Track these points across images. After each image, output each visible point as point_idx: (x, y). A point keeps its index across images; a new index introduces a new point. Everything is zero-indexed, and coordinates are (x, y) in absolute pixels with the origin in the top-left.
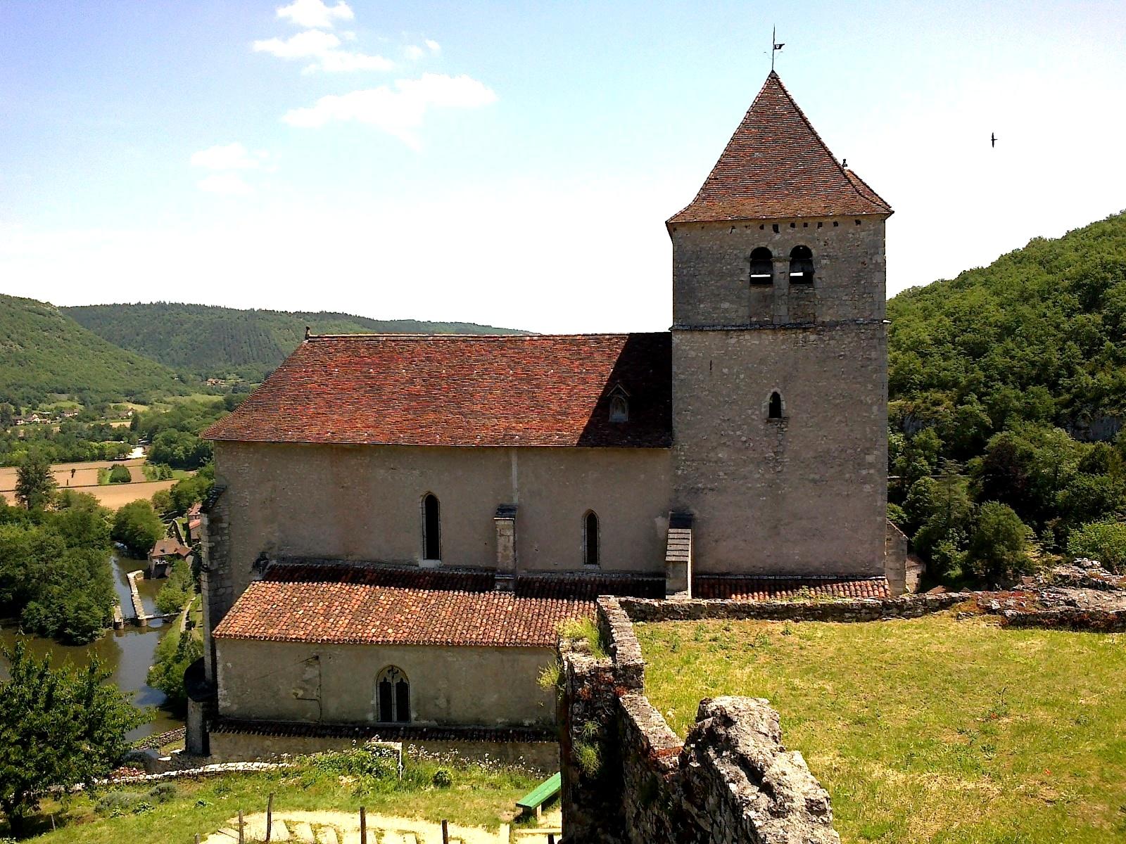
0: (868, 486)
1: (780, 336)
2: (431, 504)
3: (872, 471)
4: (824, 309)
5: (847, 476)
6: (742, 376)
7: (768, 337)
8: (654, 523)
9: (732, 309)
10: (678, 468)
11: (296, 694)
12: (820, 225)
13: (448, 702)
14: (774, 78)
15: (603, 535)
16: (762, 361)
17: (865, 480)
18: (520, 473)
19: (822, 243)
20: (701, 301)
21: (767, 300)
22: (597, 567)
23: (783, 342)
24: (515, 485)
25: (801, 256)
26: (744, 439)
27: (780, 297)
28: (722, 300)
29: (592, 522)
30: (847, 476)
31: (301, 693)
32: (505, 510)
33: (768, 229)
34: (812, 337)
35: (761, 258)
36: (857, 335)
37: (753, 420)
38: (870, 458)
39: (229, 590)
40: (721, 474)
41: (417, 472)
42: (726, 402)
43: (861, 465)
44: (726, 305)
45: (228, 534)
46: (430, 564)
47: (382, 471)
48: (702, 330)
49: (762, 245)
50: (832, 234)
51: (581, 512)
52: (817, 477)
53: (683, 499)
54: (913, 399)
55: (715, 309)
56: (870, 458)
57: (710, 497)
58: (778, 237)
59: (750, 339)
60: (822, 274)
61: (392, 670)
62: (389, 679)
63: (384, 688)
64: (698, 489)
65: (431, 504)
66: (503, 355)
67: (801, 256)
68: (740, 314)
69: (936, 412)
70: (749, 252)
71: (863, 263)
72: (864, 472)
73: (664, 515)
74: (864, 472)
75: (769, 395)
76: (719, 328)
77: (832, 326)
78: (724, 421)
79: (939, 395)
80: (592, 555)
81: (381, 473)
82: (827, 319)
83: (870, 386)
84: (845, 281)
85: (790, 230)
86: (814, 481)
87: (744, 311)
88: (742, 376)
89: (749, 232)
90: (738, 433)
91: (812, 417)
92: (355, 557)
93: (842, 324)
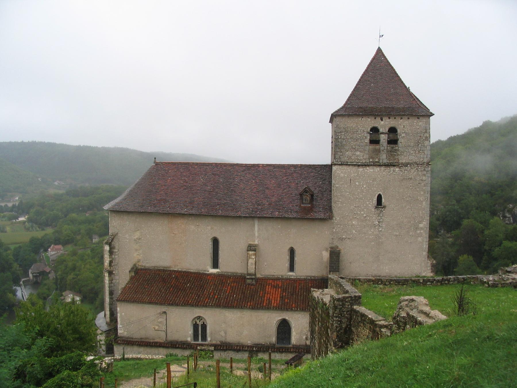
0: (420, 238)
1: (383, 168)
2: (216, 242)
3: (422, 231)
4: (403, 156)
5: (411, 233)
6: (365, 186)
7: (377, 169)
8: (321, 254)
9: (362, 156)
10: (334, 228)
11: (155, 328)
12: (401, 118)
13: (226, 333)
15: (296, 259)
16: (374, 180)
17: (420, 235)
18: (259, 229)
19: (402, 127)
21: (378, 152)
22: (294, 274)
23: (384, 171)
24: (257, 234)
25: (393, 130)
26: (365, 215)
27: (383, 151)
28: (356, 151)
29: (292, 251)
30: (411, 233)
31: (157, 328)
32: (252, 248)
34: (397, 169)
35: (375, 130)
36: (417, 169)
37: (369, 207)
38: (421, 225)
39: (117, 281)
40: (354, 231)
41: (209, 228)
42: (357, 198)
43: (417, 228)
44: (358, 153)
45: (118, 255)
46: (215, 271)
47: (193, 227)
48: (347, 165)
51: (288, 247)
52: (397, 234)
53: (336, 243)
55: (353, 154)
58: (382, 123)
59: (370, 170)
60: (402, 141)
61: (199, 318)
62: (198, 322)
63: (195, 327)
64: (343, 238)
65: (216, 242)
66: (249, 173)
67: (393, 130)
68: (365, 157)
71: (420, 136)
72: (418, 232)
73: (326, 250)
74: (418, 232)
75: (377, 195)
76: (355, 163)
77: (406, 165)
78: (356, 207)
80: (292, 268)
81: (192, 227)
82: (404, 161)
83: (422, 193)
84: (412, 144)
85: (388, 120)
86: (396, 236)
88: (365, 186)
89: (369, 120)
90: (362, 213)
91: (396, 206)
92: (178, 267)
93: (410, 164)
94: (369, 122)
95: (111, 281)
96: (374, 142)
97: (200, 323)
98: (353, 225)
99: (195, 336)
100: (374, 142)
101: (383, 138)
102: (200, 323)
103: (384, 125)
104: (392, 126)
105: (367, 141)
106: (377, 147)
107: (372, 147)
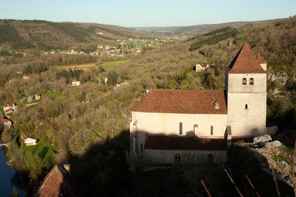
7: (245, 94)
9: (239, 89)
38: (263, 116)
43: (261, 117)
56: (263, 116)
57: (234, 123)
59: (242, 94)
61: (177, 154)
63: (176, 157)
67: (252, 79)
80: (212, 134)
87: (241, 89)
94: (243, 76)
95: (136, 140)
96: (244, 84)
97: (178, 156)
98: (236, 116)
99: (176, 162)
101: (248, 82)
102: (178, 156)
103: (248, 76)
106: (245, 86)
107: (243, 86)
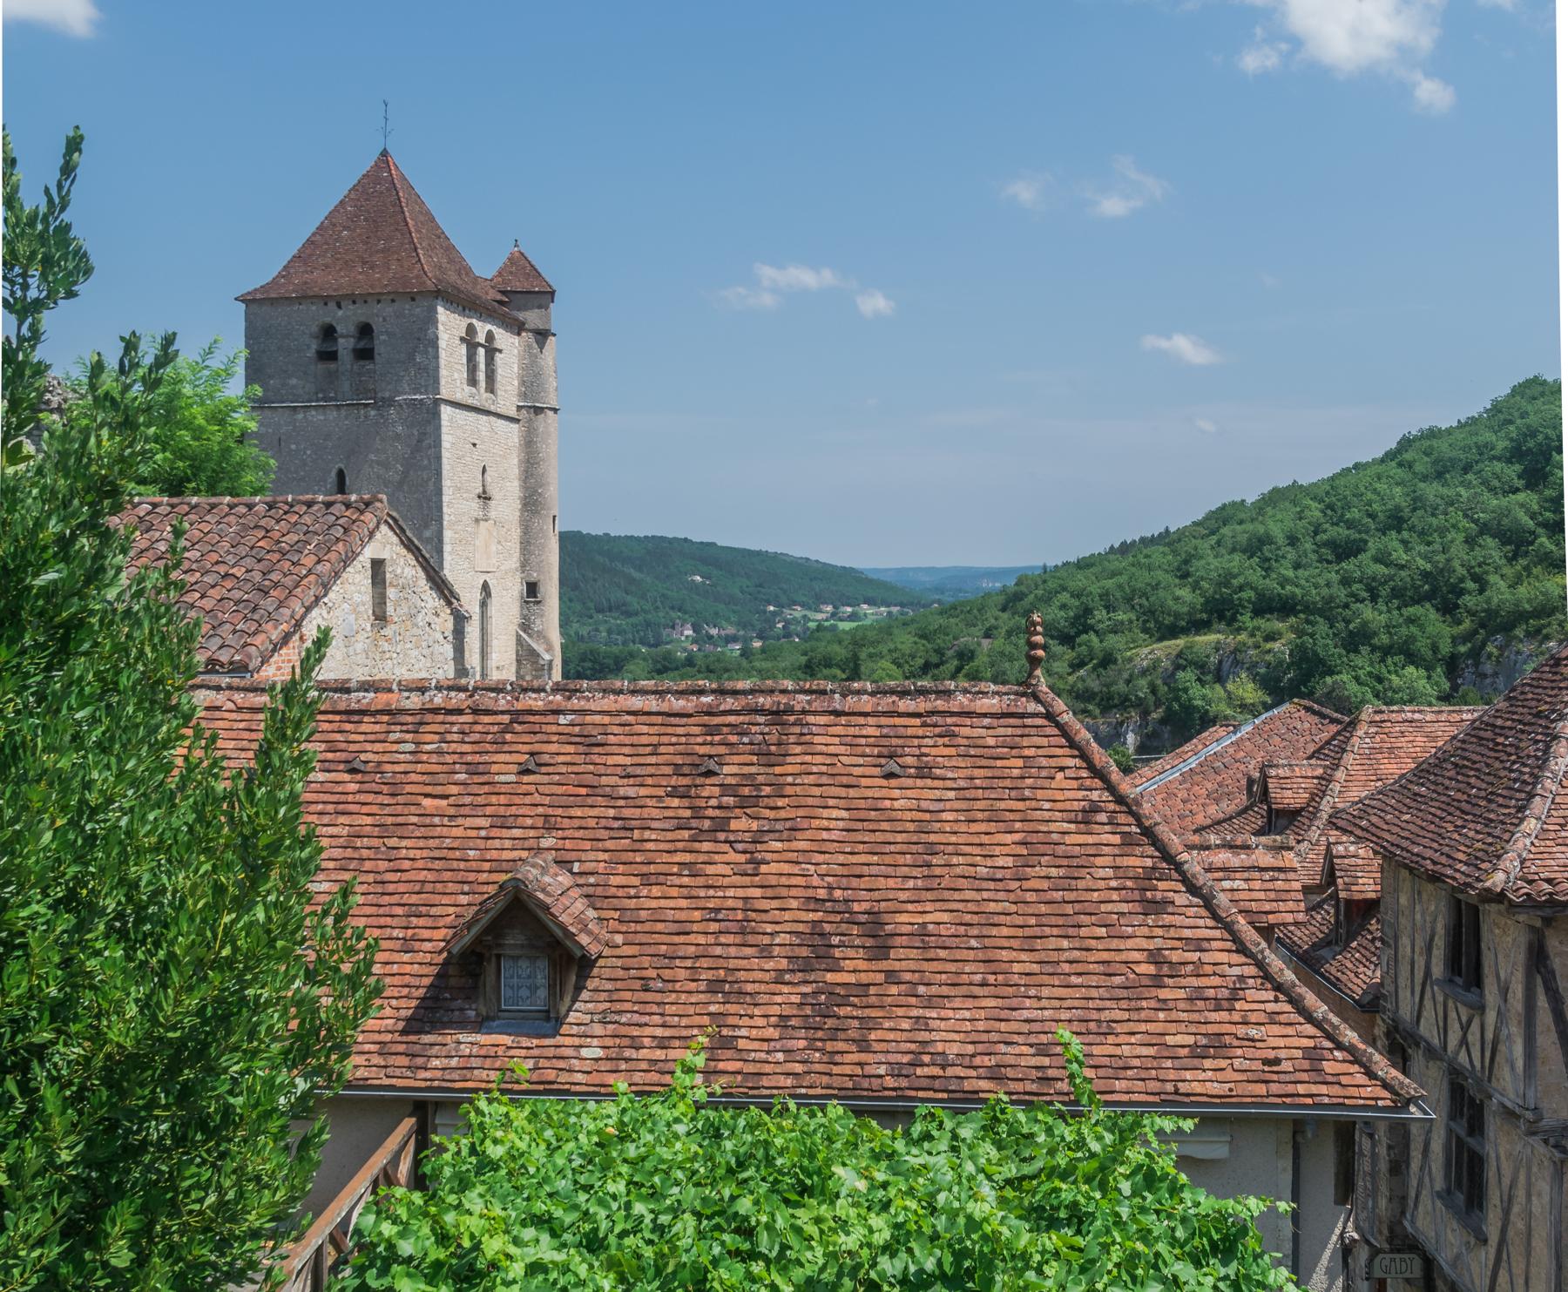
14: (385, 153)
20: (271, 377)
21: (332, 377)
33: (332, 305)
35: (329, 332)
44: (294, 381)
49: (328, 320)
50: (389, 310)
54: (1239, 630)
58: (340, 313)
60: (380, 349)
67: (365, 330)
69: (1269, 651)
70: (315, 329)
79: (1279, 625)
82: (387, 395)
96: (328, 356)
100: (328, 356)
101: (345, 345)
104: (363, 319)
105: (311, 353)
106: (332, 366)
107: (321, 367)
